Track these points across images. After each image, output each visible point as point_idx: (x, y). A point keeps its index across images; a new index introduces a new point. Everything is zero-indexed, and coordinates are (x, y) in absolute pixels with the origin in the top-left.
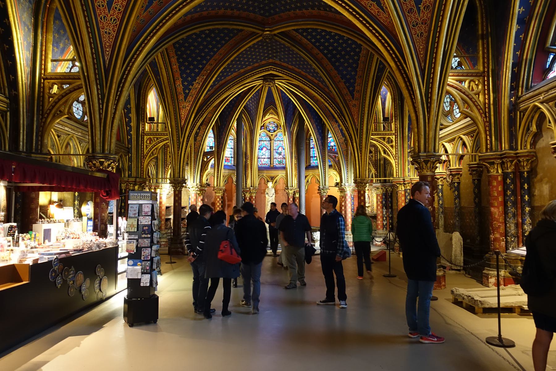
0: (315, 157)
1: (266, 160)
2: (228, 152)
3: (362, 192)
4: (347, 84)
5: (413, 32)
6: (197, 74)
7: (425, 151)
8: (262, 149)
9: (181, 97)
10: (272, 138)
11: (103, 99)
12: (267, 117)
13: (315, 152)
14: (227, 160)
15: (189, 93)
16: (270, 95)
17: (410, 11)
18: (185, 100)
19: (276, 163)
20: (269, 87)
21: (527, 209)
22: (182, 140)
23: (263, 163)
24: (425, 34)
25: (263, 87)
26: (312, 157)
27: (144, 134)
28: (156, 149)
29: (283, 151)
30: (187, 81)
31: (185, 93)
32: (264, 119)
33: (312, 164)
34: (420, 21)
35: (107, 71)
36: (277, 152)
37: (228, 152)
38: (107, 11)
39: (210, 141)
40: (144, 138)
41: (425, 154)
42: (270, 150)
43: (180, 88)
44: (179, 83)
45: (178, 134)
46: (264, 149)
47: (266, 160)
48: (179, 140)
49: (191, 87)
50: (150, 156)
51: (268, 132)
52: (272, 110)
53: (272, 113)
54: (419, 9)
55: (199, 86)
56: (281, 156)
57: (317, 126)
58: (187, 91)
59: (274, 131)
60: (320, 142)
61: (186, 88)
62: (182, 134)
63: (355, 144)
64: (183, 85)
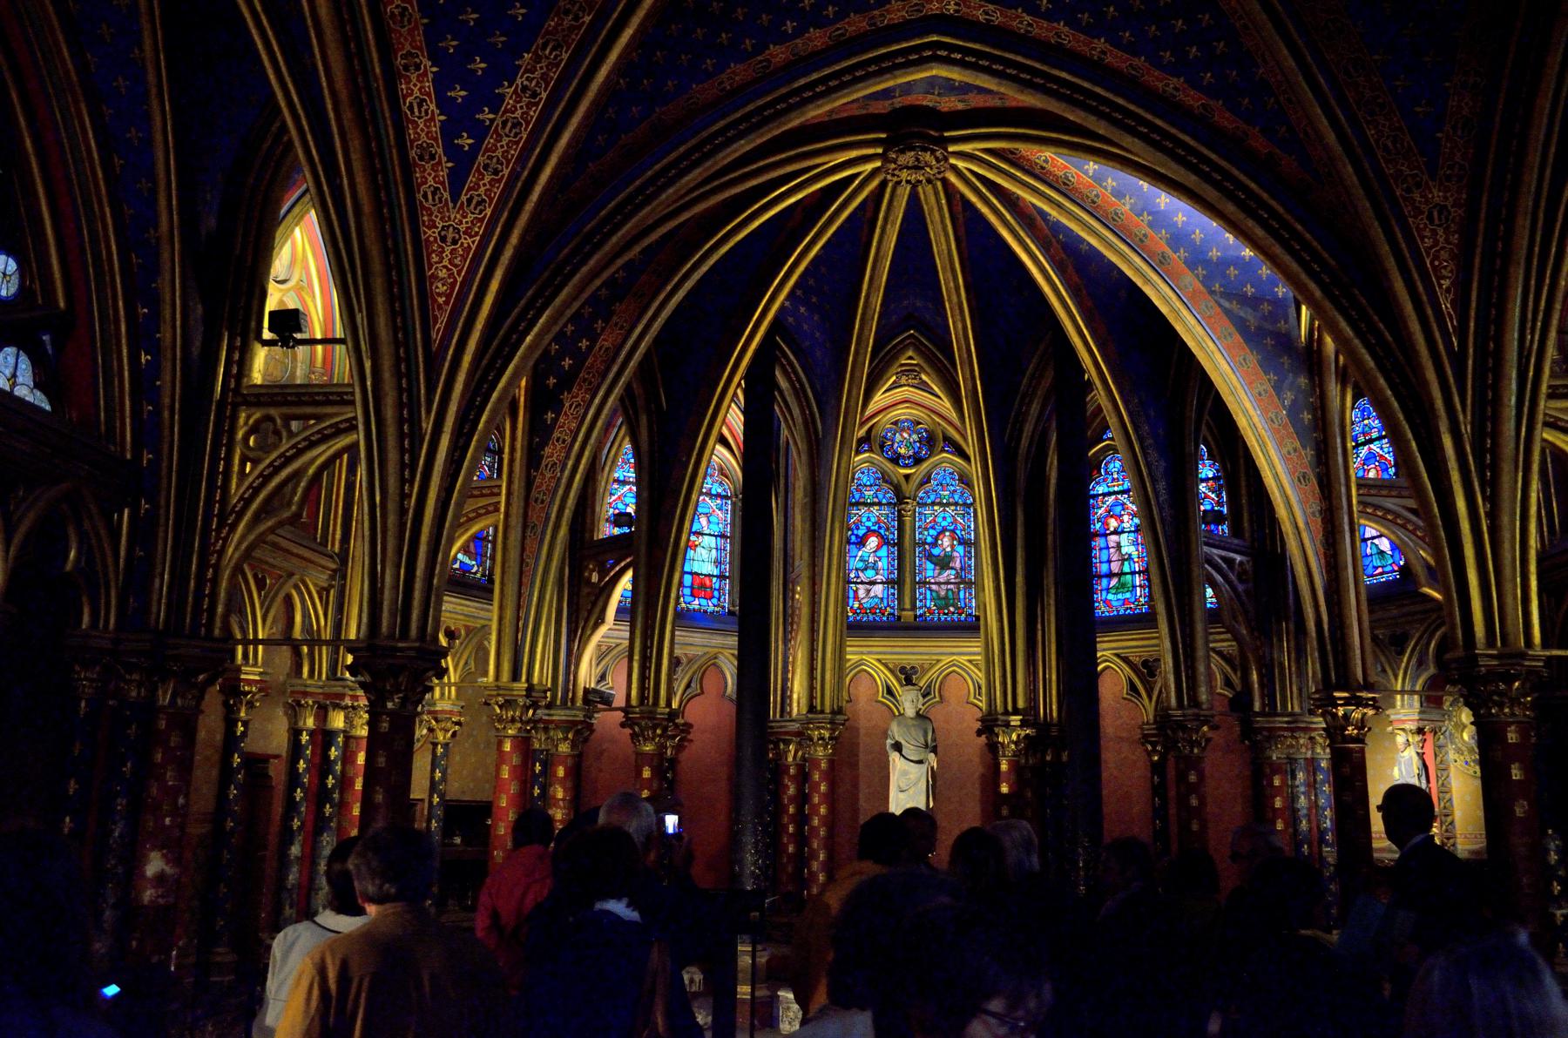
0: (1110, 575)
1: (878, 590)
6: (523, 36)
8: (861, 542)
9: (432, 176)
10: (908, 489)
12: (879, 399)
14: (703, 586)
15: (475, 149)
18: (455, 197)
19: (927, 603)
20: (915, 186)
22: (428, 426)
23: (867, 603)
26: (1101, 577)
27: (241, 394)
28: (297, 475)
29: (960, 549)
30: (468, 80)
31: (452, 151)
32: (868, 413)
36: (930, 557)
40: (234, 418)
42: (899, 544)
43: (426, 124)
44: (418, 88)
45: (412, 390)
46: (873, 542)
47: (878, 590)
48: (415, 421)
49: (486, 115)
50: (257, 519)
51: (888, 466)
52: (910, 353)
53: (909, 371)
55: (534, 114)
58: (466, 141)
59: (918, 460)
60: (1162, 485)
61: (458, 120)
64: (444, 103)
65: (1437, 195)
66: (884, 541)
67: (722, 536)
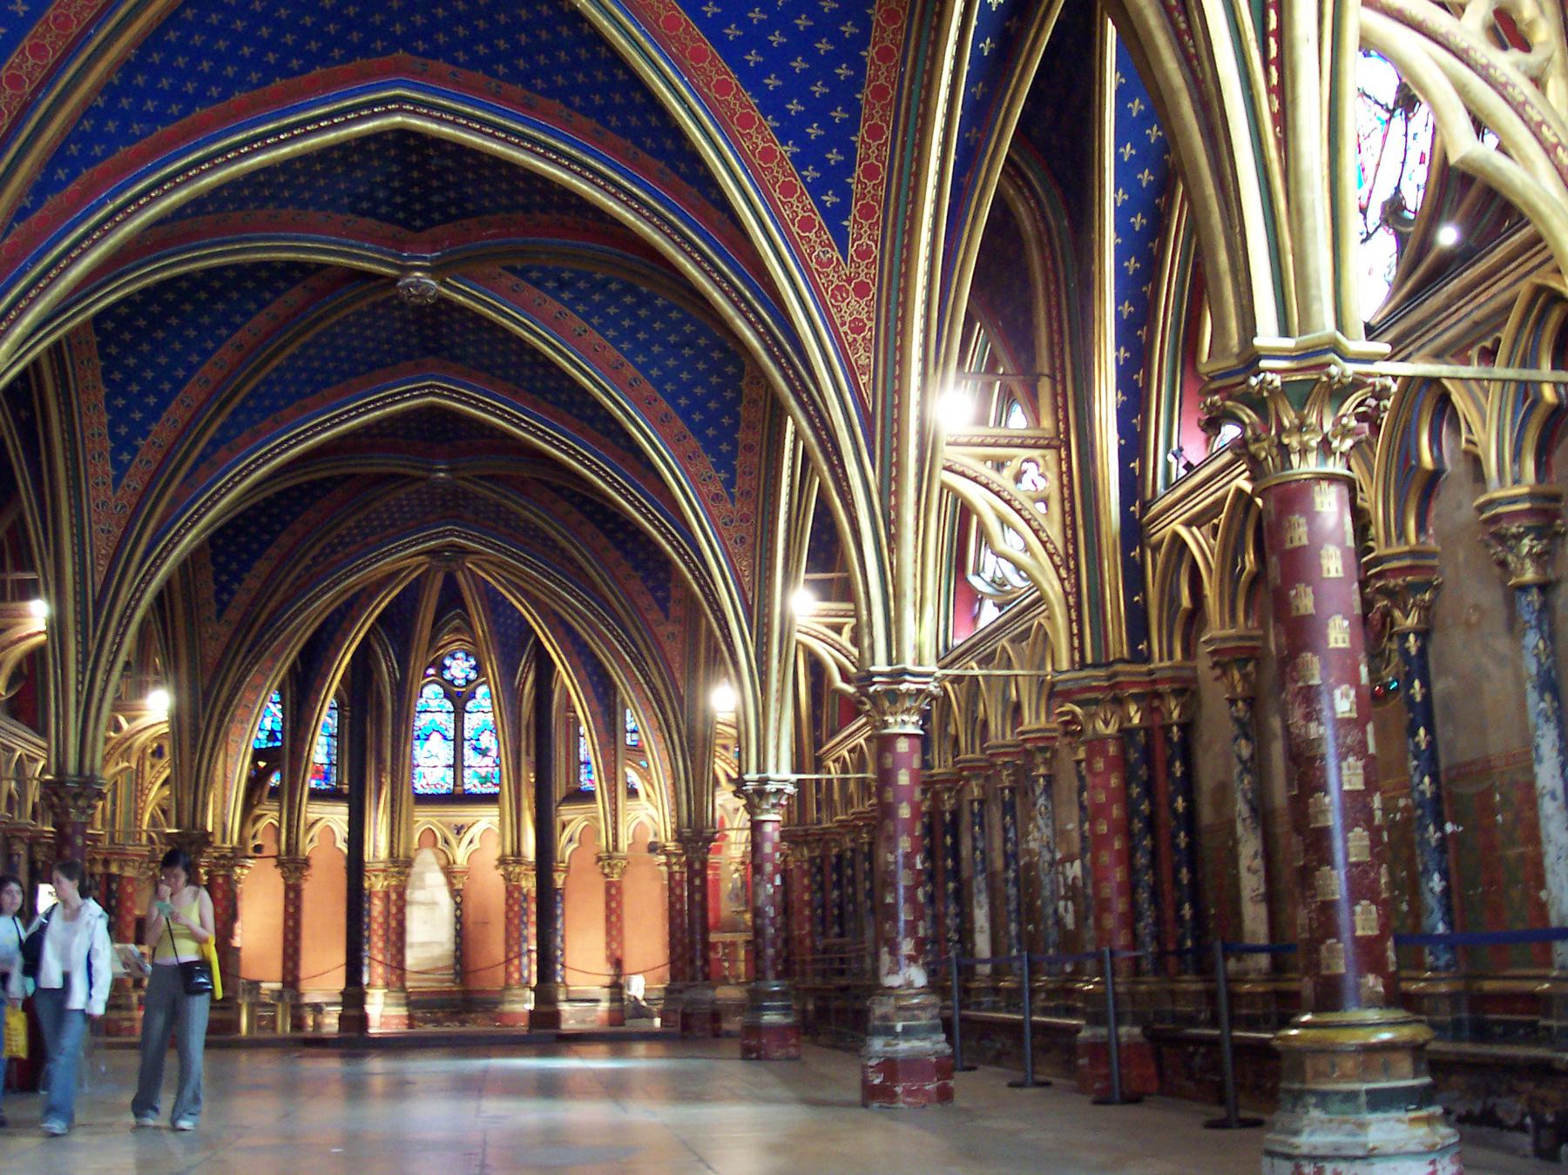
2: (320, 751)
3: (697, 866)
4: (650, 583)
5: (725, 534)
7: (759, 771)
8: (427, 738)
11: (84, 663)
13: (586, 749)
16: (450, 584)
17: (716, 497)
19: (471, 784)
21: (951, 885)
22: (203, 725)
24: (750, 541)
25: (427, 571)
31: (218, 601)
33: (586, 785)
34: (736, 516)
35: (98, 605)
36: (475, 749)
37: (320, 751)
38: (110, 493)
39: (272, 715)
41: (756, 777)
46: (436, 737)
53: (457, 630)
54: (732, 496)
56: (488, 761)
57: (589, 676)
58: (225, 597)
61: (222, 588)
62: (205, 708)
63: (675, 737)
65: (670, 629)
66: (445, 738)
67: (331, 736)
